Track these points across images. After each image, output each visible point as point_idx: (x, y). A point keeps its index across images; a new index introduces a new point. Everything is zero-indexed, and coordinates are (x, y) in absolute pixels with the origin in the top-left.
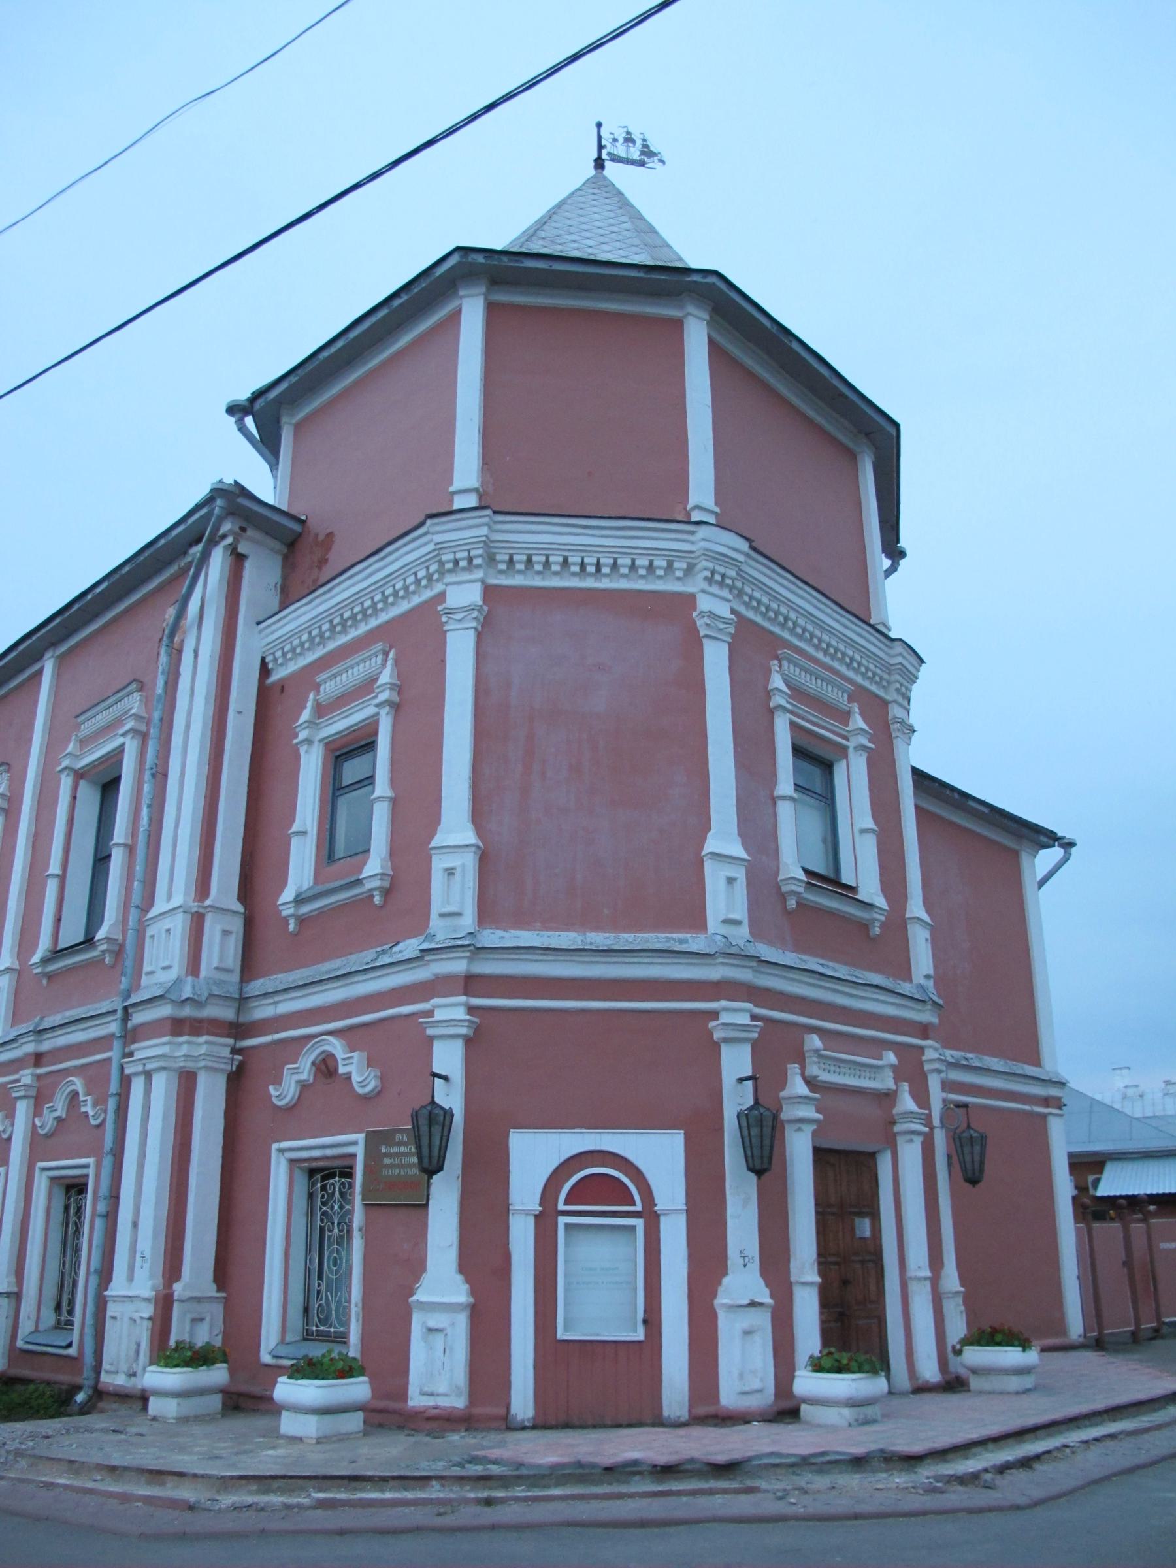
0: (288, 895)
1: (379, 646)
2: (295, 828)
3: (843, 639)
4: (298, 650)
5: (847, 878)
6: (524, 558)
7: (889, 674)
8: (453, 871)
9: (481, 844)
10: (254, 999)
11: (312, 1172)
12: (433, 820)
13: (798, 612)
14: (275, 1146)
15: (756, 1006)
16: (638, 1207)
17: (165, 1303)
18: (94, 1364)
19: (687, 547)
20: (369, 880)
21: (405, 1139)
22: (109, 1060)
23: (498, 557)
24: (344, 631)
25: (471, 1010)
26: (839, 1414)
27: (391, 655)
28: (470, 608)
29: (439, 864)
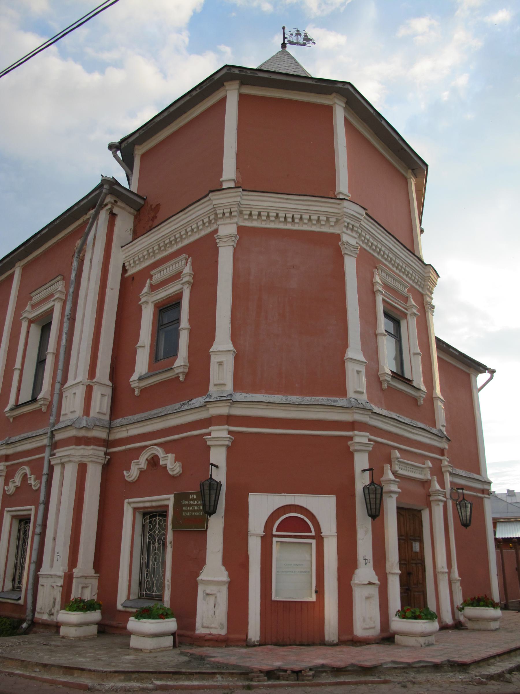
0: (135, 377)
1: (184, 255)
2: (139, 344)
3: (404, 261)
4: (142, 260)
5: (407, 375)
6: (257, 213)
7: (424, 281)
8: (222, 363)
9: (235, 351)
10: (116, 428)
11: (144, 514)
12: (211, 338)
13: (386, 247)
14: (126, 501)
15: (371, 435)
16: (313, 534)
17: (69, 578)
18: (32, 608)
19: (336, 211)
20: (177, 368)
21: (195, 497)
22: (43, 458)
23: (244, 212)
24: (165, 250)
25: (230, 432)
26: (416, 640)
27: (190, 260)
28: (230, 236)
29: (214, 360)
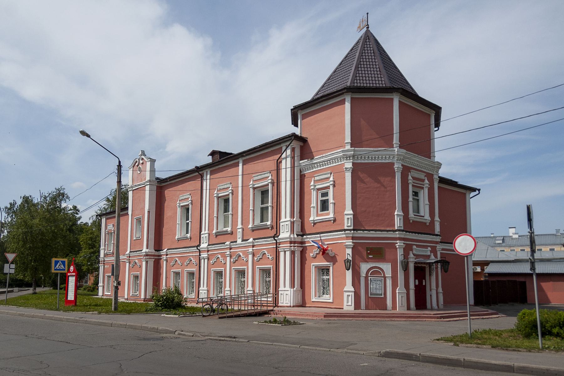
16: (383, 276)
25: (353, 243)
